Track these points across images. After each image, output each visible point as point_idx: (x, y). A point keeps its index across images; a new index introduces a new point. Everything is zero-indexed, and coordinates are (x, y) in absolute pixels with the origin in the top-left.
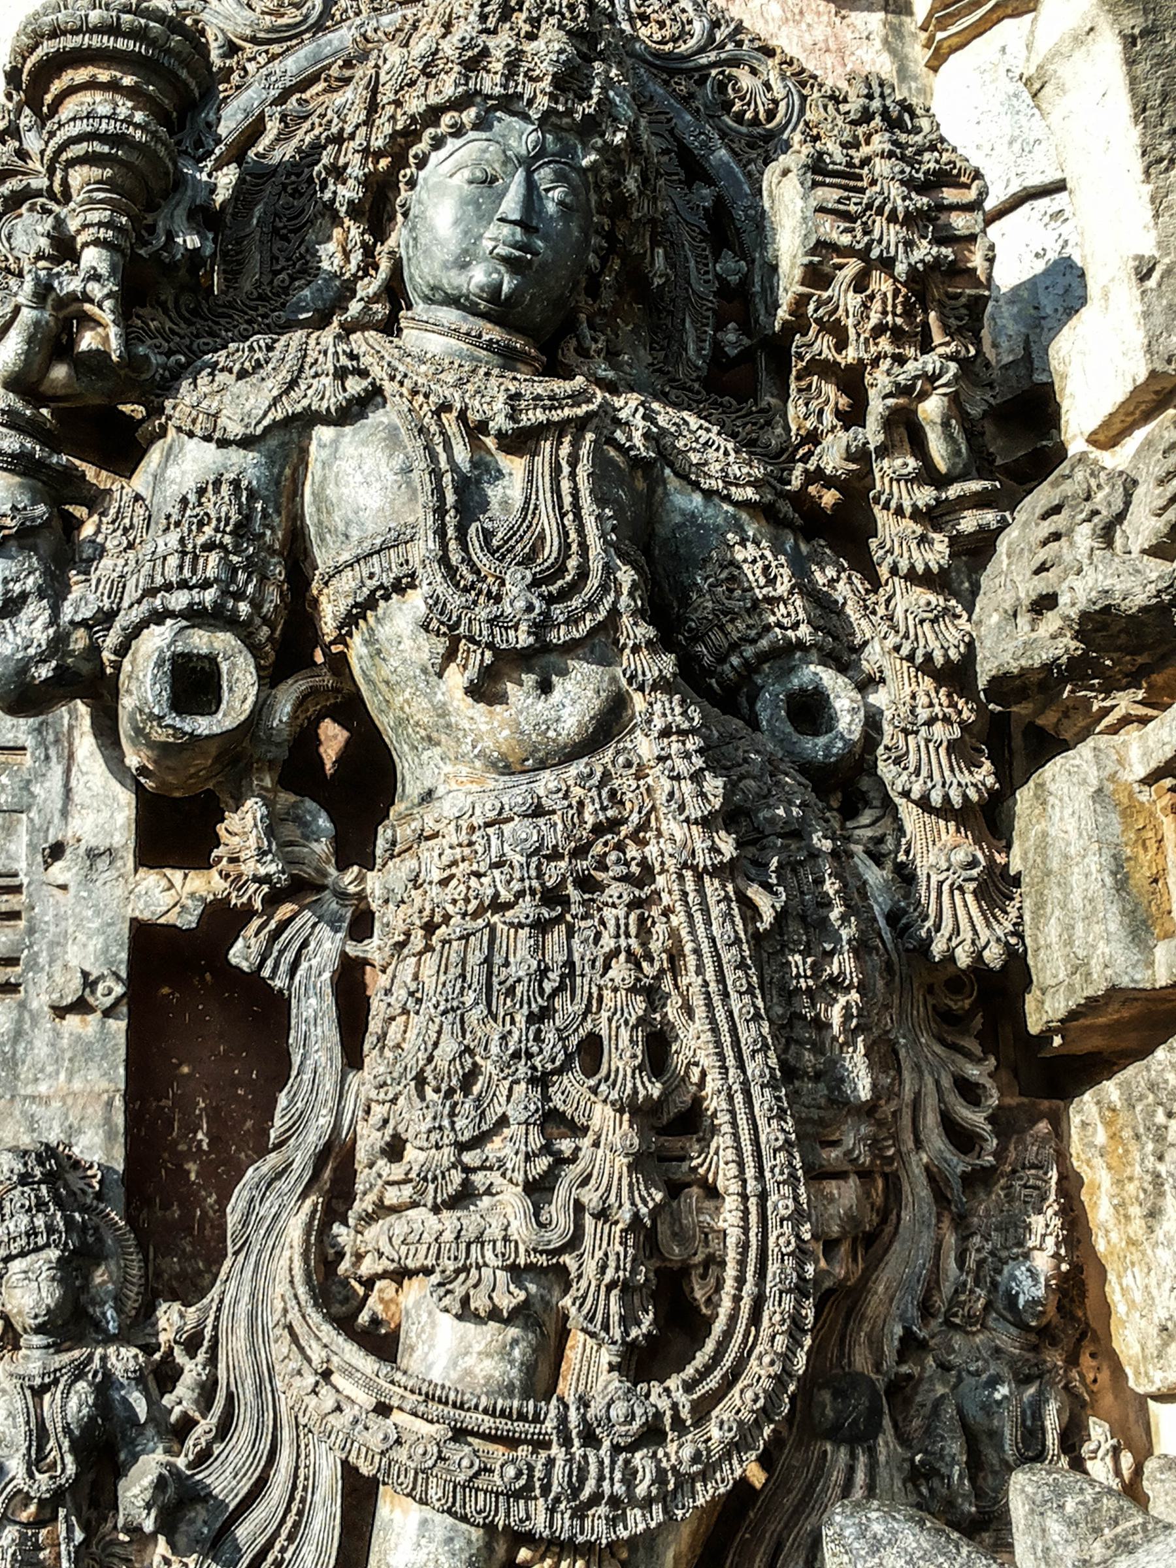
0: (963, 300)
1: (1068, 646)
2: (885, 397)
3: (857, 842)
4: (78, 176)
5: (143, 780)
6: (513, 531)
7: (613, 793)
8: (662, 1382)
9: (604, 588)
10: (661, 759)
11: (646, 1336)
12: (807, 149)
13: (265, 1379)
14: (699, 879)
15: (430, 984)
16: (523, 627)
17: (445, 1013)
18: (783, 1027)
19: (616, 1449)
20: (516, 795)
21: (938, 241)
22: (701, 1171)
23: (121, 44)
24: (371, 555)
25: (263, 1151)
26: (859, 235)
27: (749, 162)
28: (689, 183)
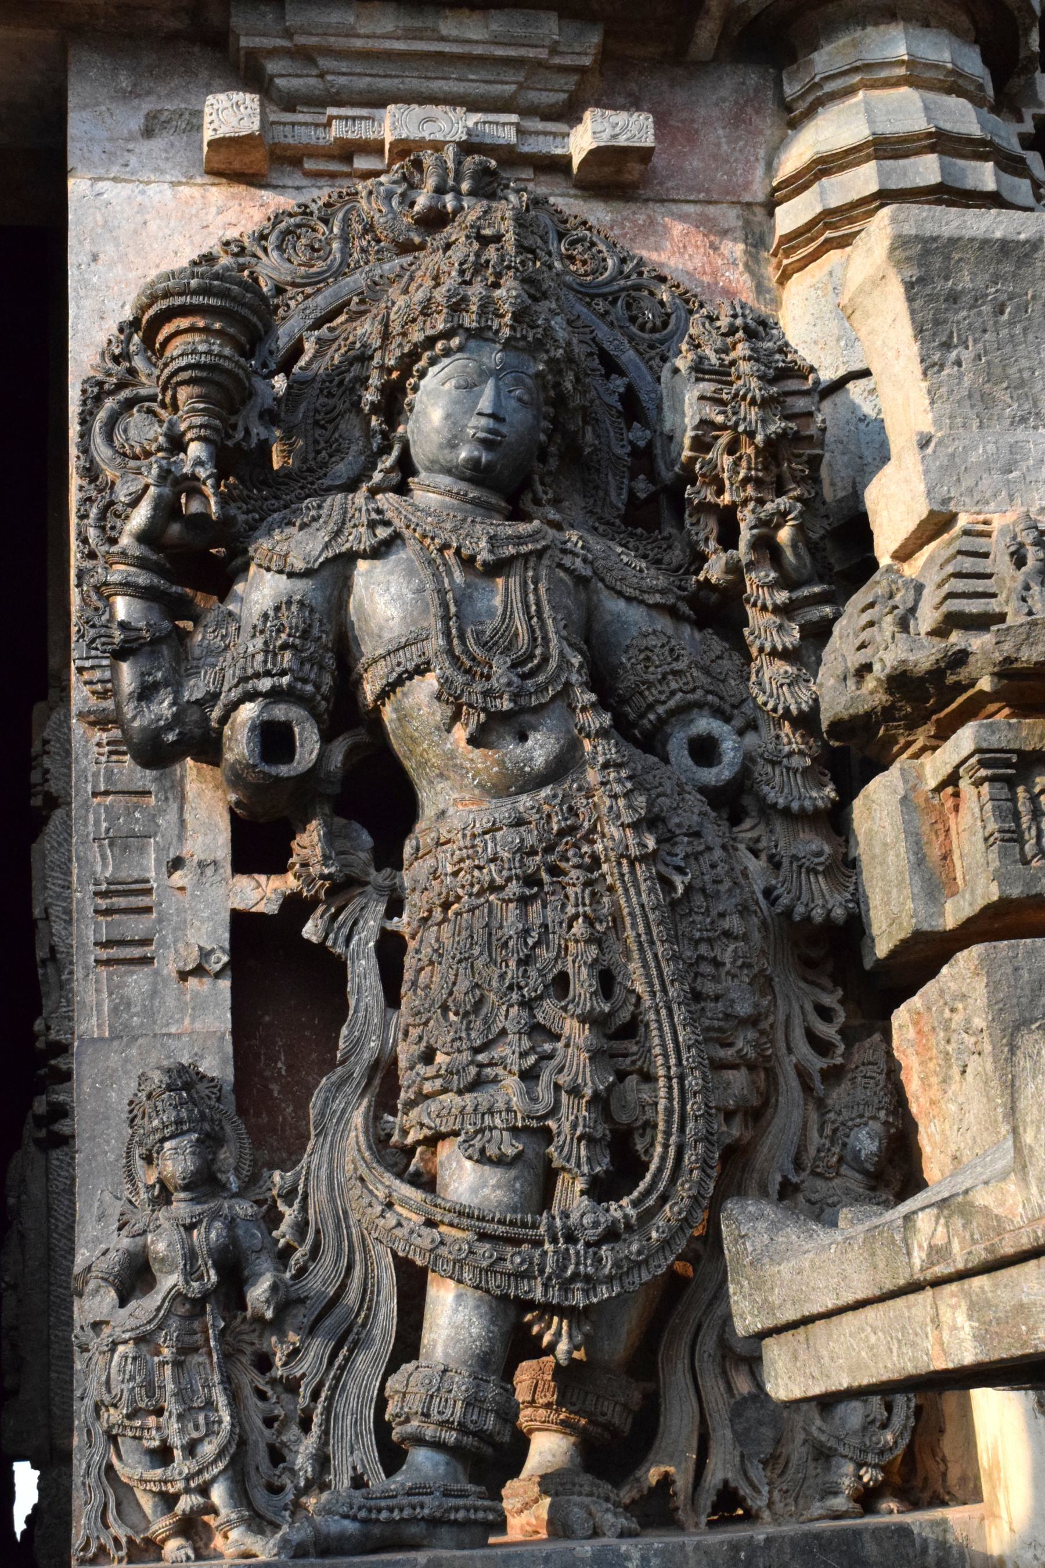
0: (805, 458)
1: (881, 698)
2: (751, 528)
3: (741, 842)
4: (183, 393)
5: (238, 811)
6: (496, 630)
7: (571, 809)
8: (617, 1201)
9: (559, 667)
10: (603, 784)
11: (606, 1172)
12: (691, 356)
13: (341, 1220)
14: (632, 864)
15: (448, 943)
16: (506, 696)
17: (460, 961)
18: (692, 965)
19: (588, 1245)
20: (503, 811)
21: (787, 417)
22: (639, 1063)
23: (212, 301)
24: (398, 650)
25: (332, 1065)
26: (730, 414)
27: (651, 359)
28: (607, 376)
